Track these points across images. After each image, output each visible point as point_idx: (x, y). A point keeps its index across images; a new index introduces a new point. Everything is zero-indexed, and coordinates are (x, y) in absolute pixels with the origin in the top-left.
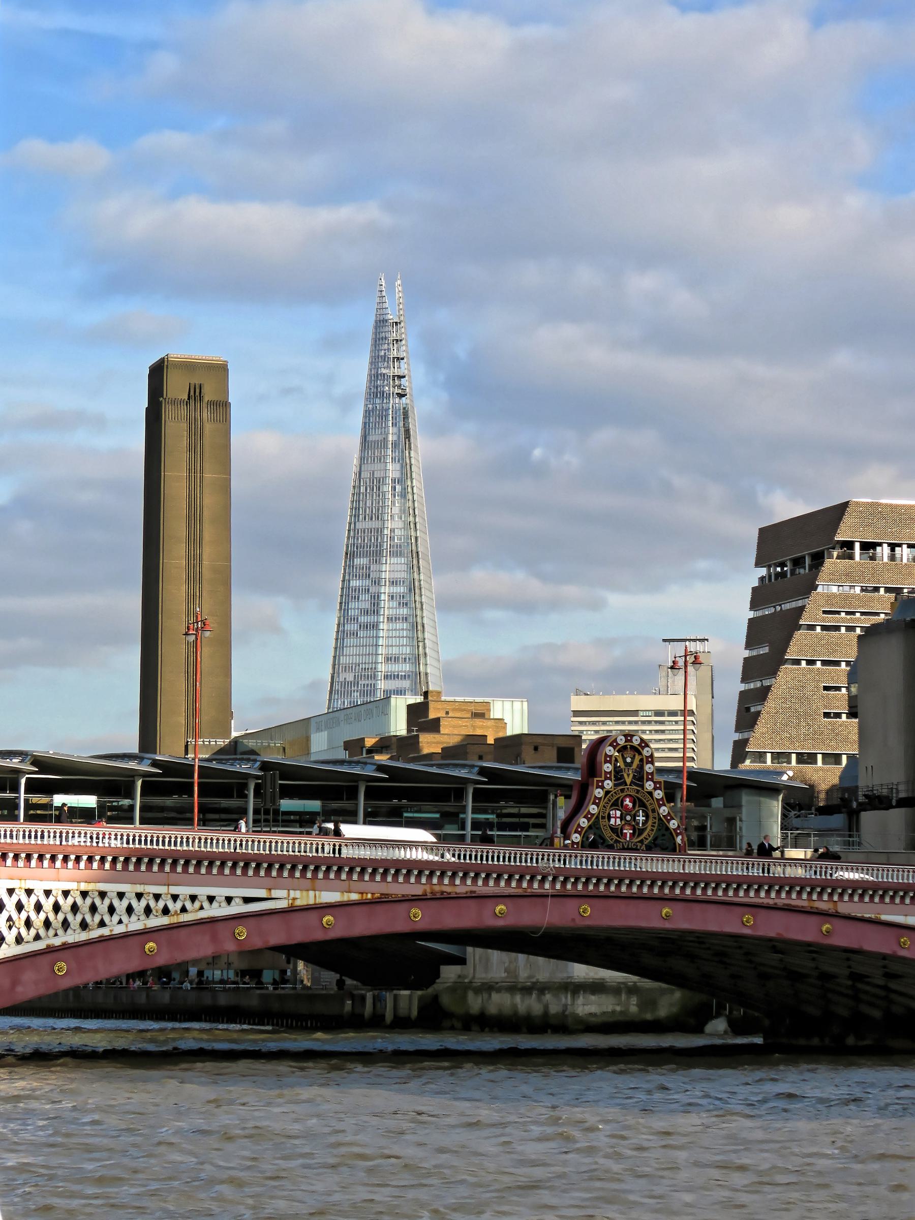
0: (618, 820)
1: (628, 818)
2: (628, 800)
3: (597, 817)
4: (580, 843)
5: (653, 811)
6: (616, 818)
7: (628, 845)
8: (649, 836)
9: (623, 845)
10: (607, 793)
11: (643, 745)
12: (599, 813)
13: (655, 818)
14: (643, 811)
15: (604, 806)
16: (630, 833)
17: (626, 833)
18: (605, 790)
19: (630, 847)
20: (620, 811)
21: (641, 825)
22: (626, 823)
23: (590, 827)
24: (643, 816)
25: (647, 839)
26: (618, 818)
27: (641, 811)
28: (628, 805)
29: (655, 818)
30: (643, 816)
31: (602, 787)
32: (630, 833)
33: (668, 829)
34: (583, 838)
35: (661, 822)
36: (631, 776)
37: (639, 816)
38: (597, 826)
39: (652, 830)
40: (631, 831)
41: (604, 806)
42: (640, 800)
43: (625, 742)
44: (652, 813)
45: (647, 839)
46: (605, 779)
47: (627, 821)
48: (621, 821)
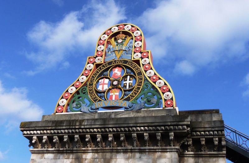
3: (86, 84)
4: (65, 106)
6: (104, 84)
10: (97, 66)
12: (88, 81)
14: (131, 76)
16: (116, 95)
18: (95, 64)
20: (109, 79)
21: (128, 87)
23: (77, 92)
24: (130, 80)
27: (128, 77)
32: (116, 95)
35: (146, 82)
37: (126, 80)
38: (84, 92)
41: (93, 77)
43: (118, 30)
44: (138, 76)
46: (97, 57)
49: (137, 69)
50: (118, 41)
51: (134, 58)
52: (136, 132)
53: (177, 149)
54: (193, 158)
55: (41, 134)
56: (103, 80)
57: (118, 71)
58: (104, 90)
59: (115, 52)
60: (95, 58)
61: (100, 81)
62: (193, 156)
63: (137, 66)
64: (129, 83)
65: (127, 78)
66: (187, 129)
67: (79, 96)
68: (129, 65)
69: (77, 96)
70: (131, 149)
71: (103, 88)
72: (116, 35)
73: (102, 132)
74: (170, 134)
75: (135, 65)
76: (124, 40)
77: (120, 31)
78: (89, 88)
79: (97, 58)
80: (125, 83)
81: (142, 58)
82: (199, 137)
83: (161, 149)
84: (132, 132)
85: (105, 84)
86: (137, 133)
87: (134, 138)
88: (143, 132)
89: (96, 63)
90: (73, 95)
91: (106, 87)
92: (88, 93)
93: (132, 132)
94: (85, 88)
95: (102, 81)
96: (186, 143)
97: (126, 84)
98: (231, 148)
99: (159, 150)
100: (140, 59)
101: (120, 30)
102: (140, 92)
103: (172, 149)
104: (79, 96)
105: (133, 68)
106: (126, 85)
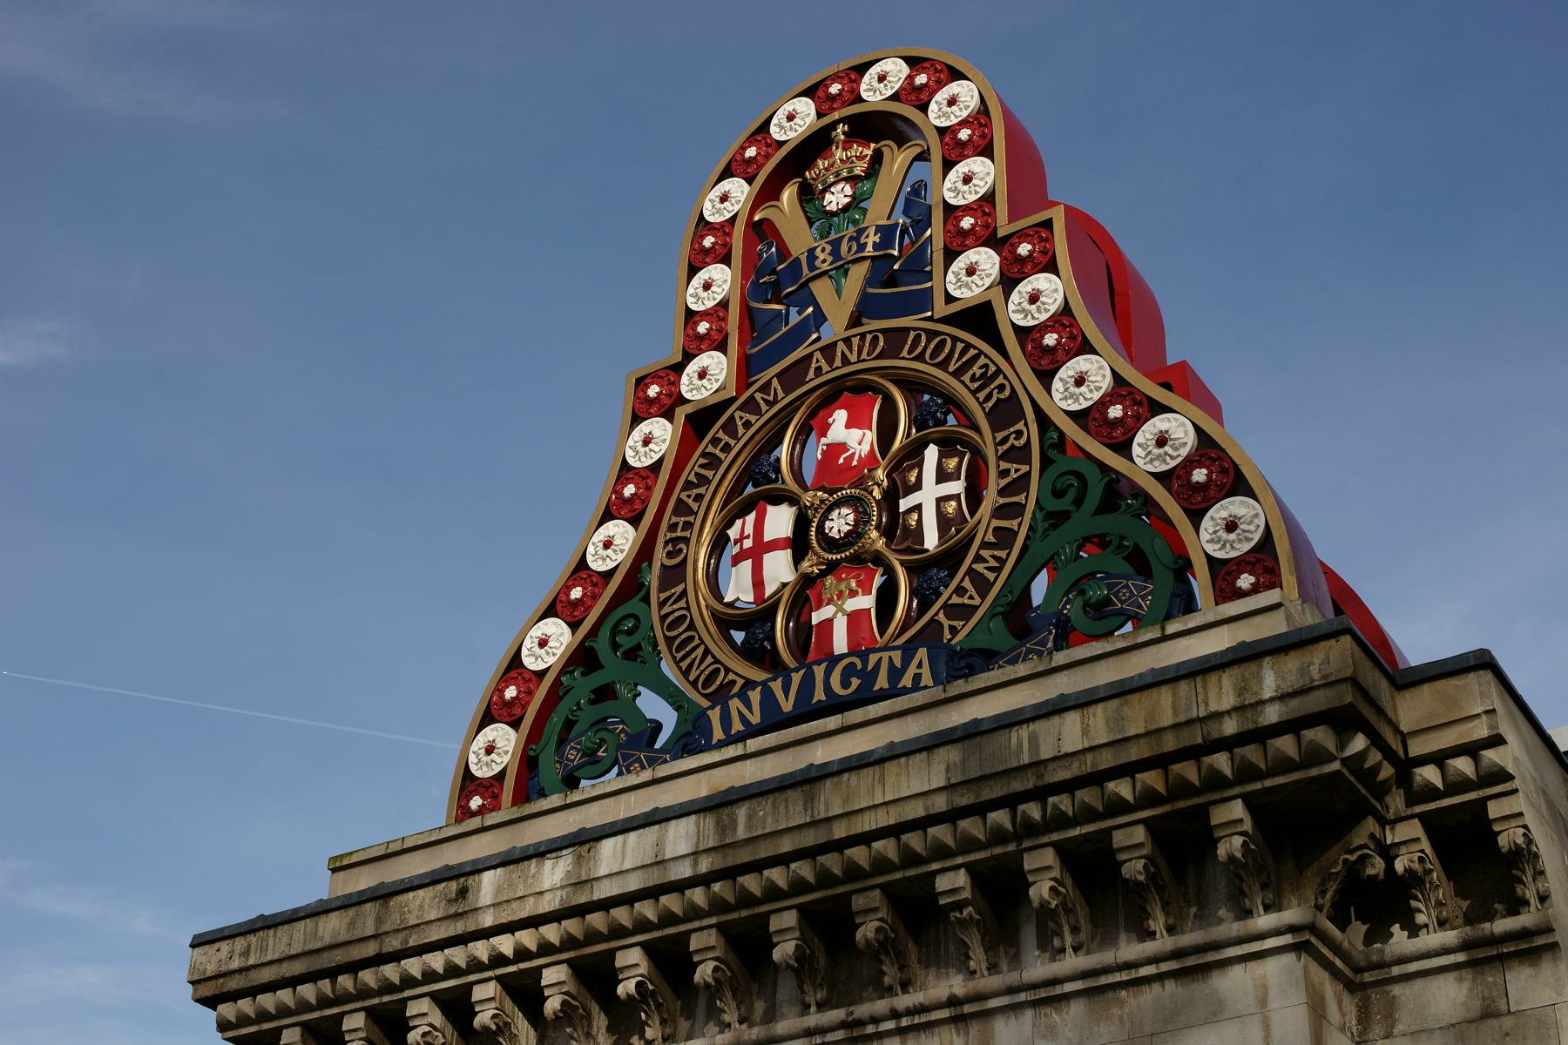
0: (779, 569)
1: (840, 523)
2: (841, 416)
5: (1006, 412)
6: (761, 548)
7: (808, 684)
8: (983, 586)
9: (768, 696)
11: (921, 79)
12: (644, 553)
13: (1020, 454)
14: (948, 445)
15: (682, 509)
16: (855, 618)
17: (828, 624)
18: (681, 413)
19: (819, 695)
20: (792, 500)
21: (931, 540)
22: (832, 567)
24: (942, 476)
25: (970, 610)
26: (774, 545)
28: (843, 447)
29: (1020, 454)
30: (942, 476)
31: (667, 407)
32: (855, 618)
33: (1117, 491)
34: (534, 736)
36: (859, 272)
38: (626, 642)
39: (1004, 538)
40: (866, 602)
42: (912, 386)
43: (820, 115)
44: (994, 429)
45: (965, 612)
46: (688, 357)
47: (830, 544)
48: (797, 560)
49: (986, 379)
50: (828, 197)
51: (950, 299)
52: (960, 860)
53: (1292, 929)
54: (1460, 980)
55: (324, 1002)
56: (751, 518)
57: (848, 426)
58: (769, 591)
59: (814, 286)
60: (679, 368)
61: (733, 533)
62: (1460, 957)
63: (981, 353)
64: (940, 501)
65: (920, 465)
66: (1342, 746)
67: (598, 679)
68: (920, 358)
69: (584, 685)
70: (953, 1001)
71: (758, 583)
72: (810, 164)
73: (718, 906)
74: (1219, 815)
75: (968, 346)
76: (867, 185)
77: (833, 126)
78: (662, 604)
79: (693, 368)
80: (910, 511)
81: (1008, 282)
82: (1472, 796)
83: (1177, 954)
84: (935, 866)
85: (774, 545)
86: (968, 866)
87: (959, 906)
88: (1011, 847)
89: (688, 409)
90: (557, 682)
91: (779, 569)
92: (662, 646)
93: (935, 866)
94: (634, 616)
95: (749, 530)
96: (1377, 867)
97: (915, 516)
98: (1403, 800)
99: (1165, 967)
100: (996, 297)
101: (836, 115)
102: (1025, 548)
103: (1262, 936)
104: (598, 679)
105: (957, 374)
106: (920, 521)
